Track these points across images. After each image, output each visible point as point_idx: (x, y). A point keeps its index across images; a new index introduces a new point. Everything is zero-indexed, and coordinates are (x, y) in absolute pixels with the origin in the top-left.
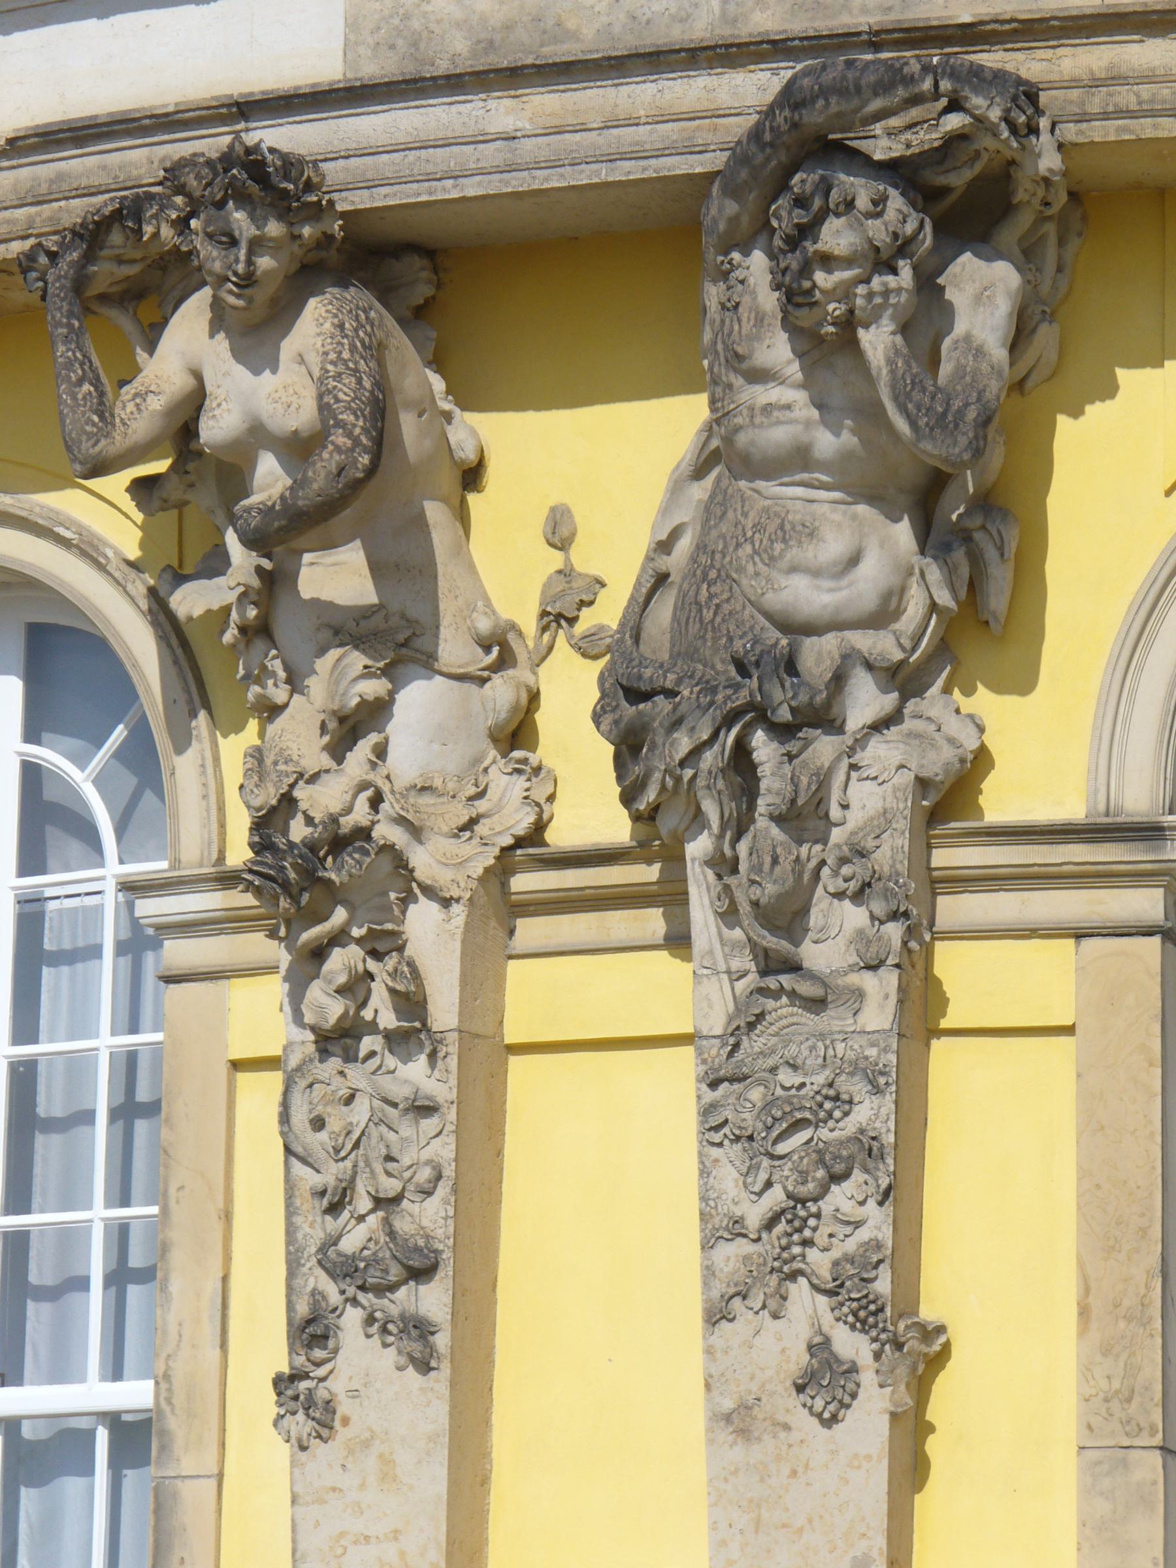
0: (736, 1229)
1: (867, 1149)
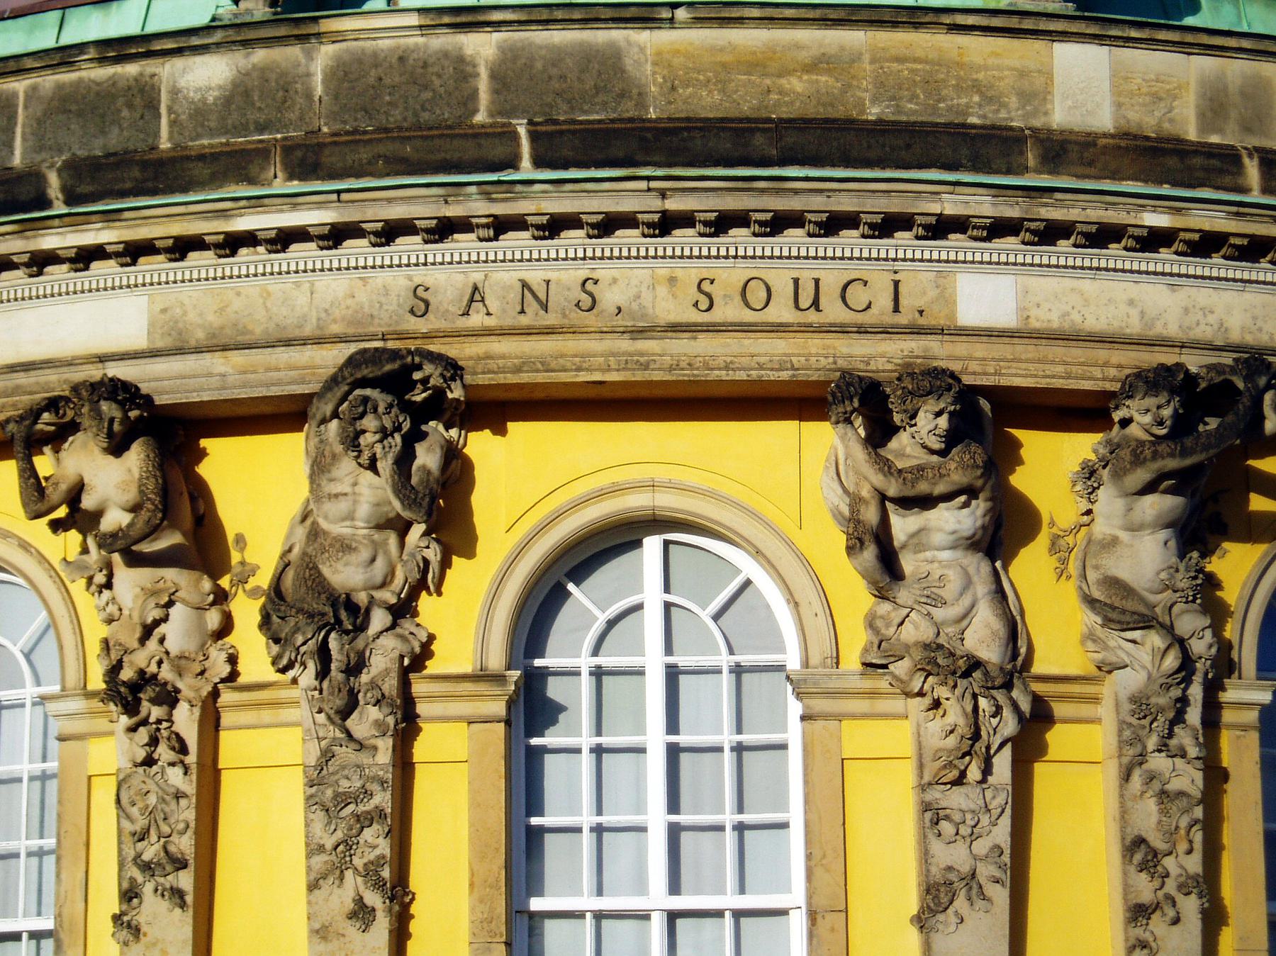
0: (321, 849)
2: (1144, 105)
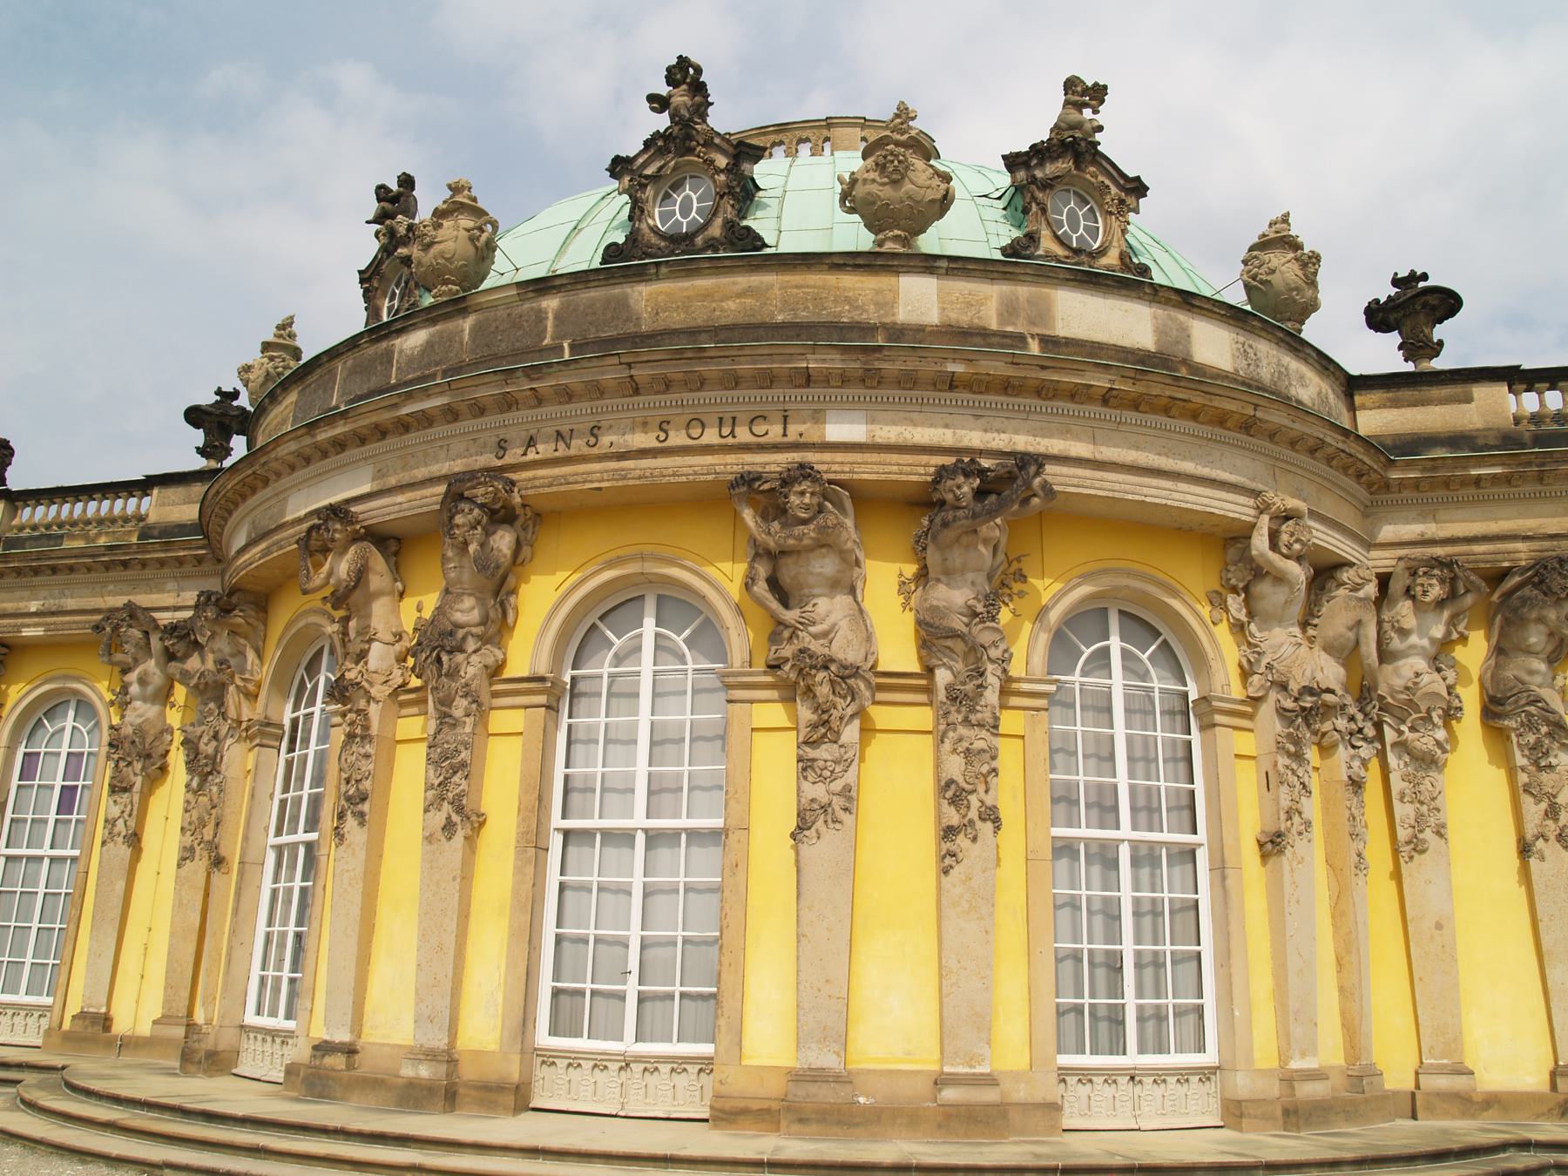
0: (432, 787)
1: (463, 765)
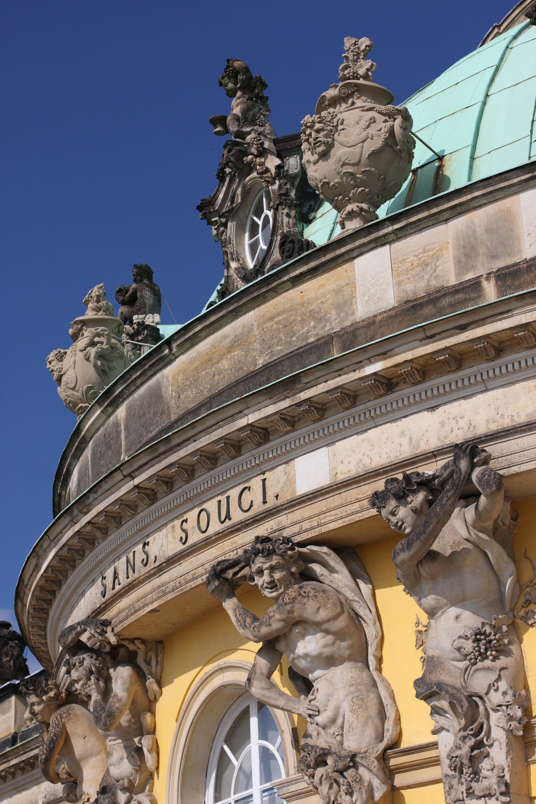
2: (414, 276)
